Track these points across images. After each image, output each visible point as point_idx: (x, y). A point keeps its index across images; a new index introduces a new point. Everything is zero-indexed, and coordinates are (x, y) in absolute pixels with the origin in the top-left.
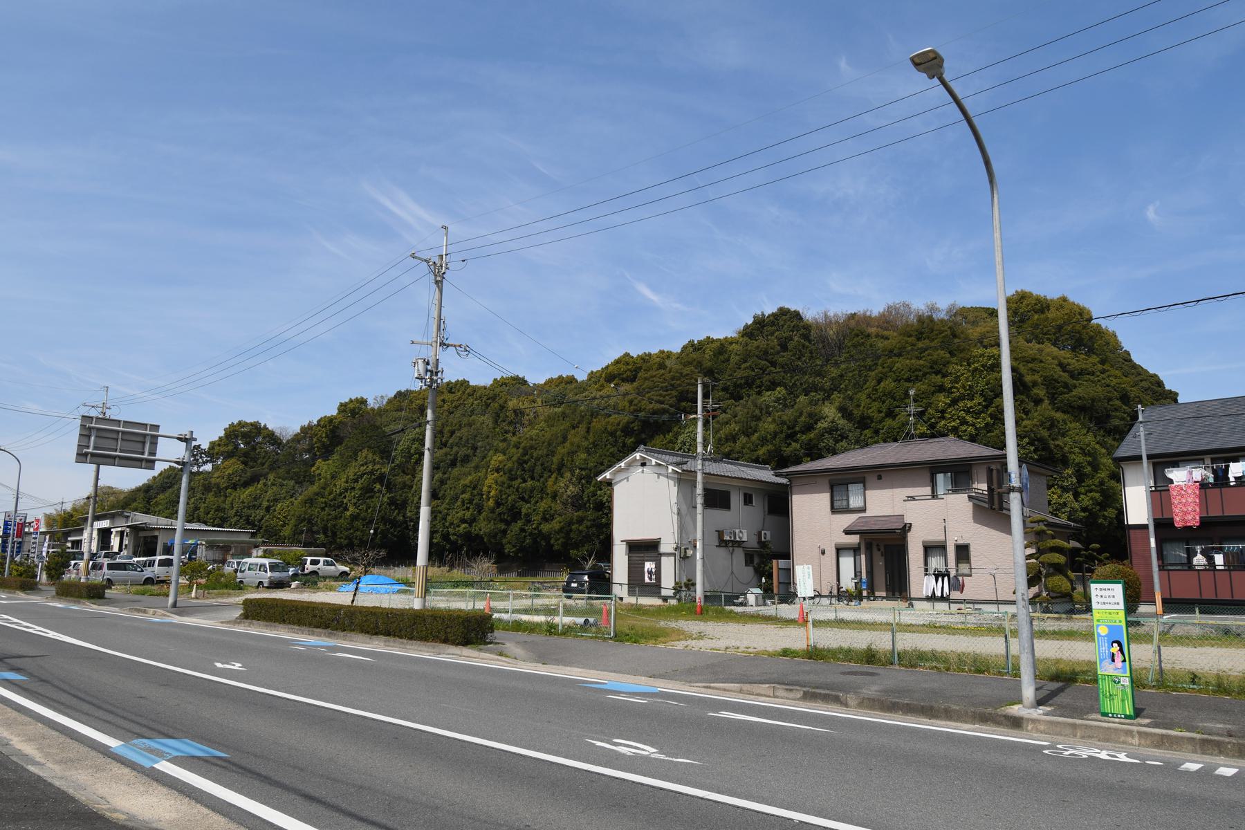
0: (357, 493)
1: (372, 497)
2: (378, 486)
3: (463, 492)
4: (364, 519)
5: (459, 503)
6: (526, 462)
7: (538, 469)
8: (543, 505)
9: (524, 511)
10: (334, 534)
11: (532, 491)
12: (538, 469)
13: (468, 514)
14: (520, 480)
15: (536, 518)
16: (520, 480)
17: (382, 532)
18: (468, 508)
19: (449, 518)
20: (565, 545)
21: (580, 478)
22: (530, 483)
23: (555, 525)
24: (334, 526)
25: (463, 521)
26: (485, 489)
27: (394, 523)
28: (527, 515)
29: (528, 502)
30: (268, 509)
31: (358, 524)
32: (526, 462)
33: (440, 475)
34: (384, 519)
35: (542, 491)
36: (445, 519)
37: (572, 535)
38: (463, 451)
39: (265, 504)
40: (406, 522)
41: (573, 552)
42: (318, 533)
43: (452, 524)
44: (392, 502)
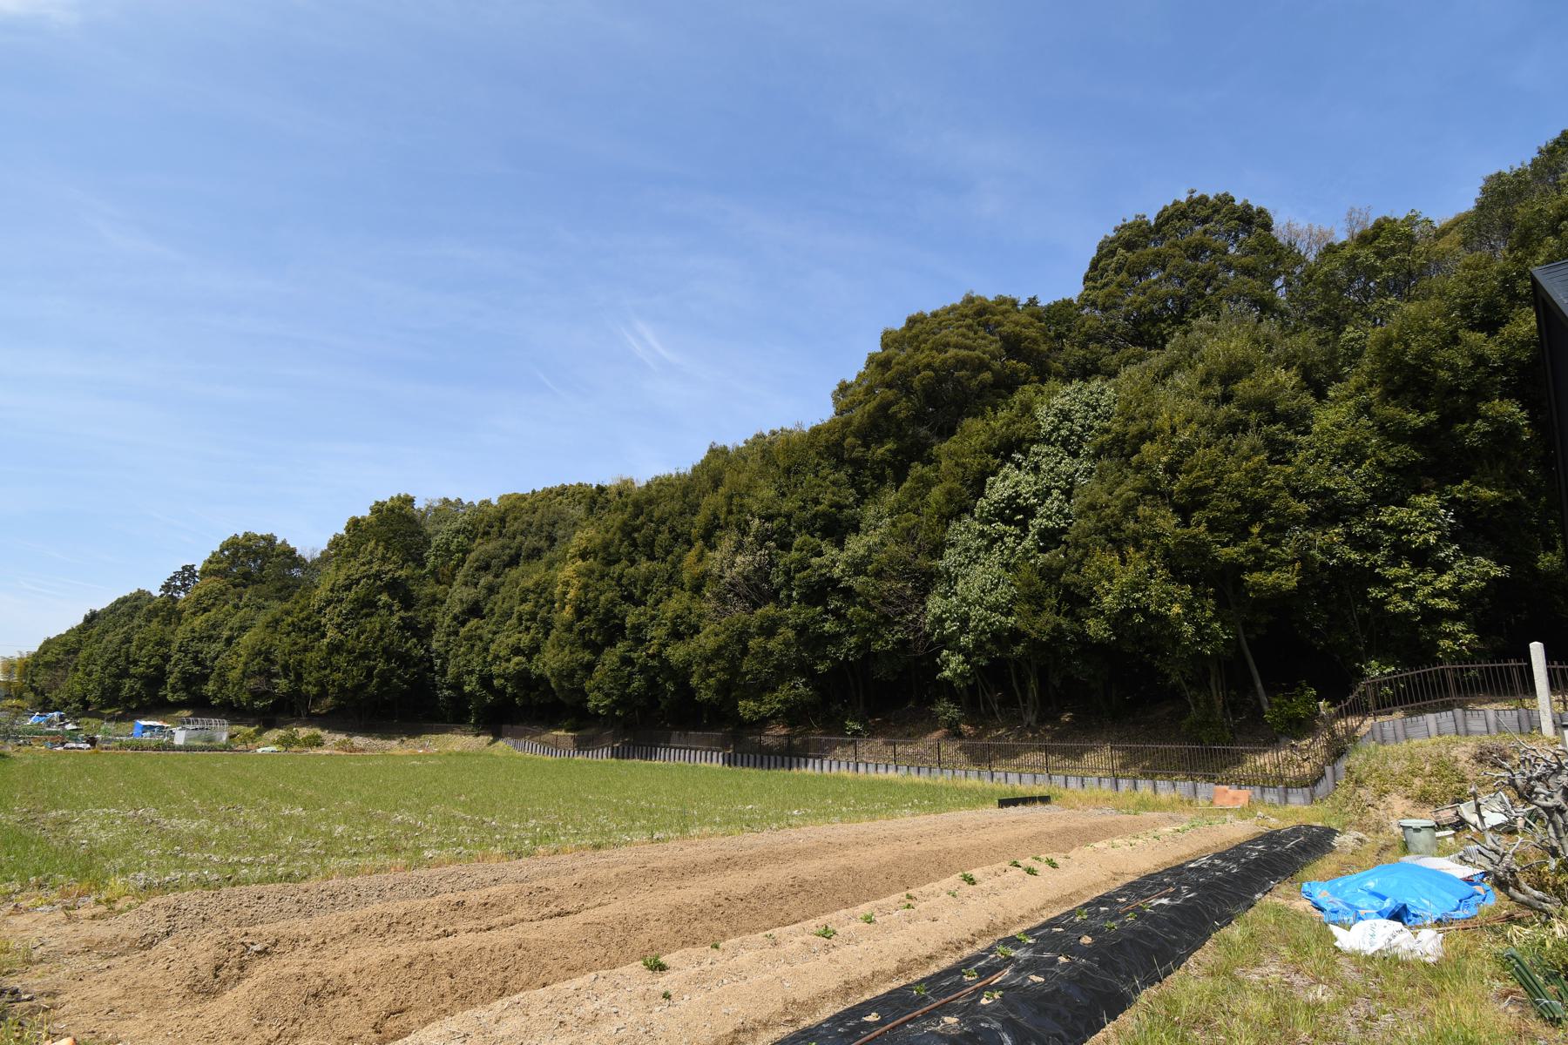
0: (345, 607)
1: (371, 615)
2: (384, 597)
3: (523, 601)
4: (350, 652)
5: (514, 620)
6: (637, 529)
7: (664, 537)
8: (672, 606)
9: (630, 621)
10: (299, 677)
11: (648, 581)
12: (664, 537)
13: (526, 639)
14: (624, 562)
15: (657, 633)
16: (624, 562)
17: (382, 672)
18: (528, 629)
19: (493, 647)
20: (725, 689)
21: (762, 539)
22: (644, 566)
23: (706, 640)
24: (300, 662)
25: (517, 651)
26: (557, 591)
27: (405, 660)
28: (638, 628)
29: (638, 603)
30: (229, 641)
31: (340, 660)
32: (637, 529)
33: (490, 578)
34: (388, 653)
35: (672, 579)
36: (486, 650)
37: (747, 664)
38: (531, 542)
39: (226, 634)
40: (430, 660)
41: (746, 707)
42: (276, 675)
43: (496, 657)
44: (407, 626)
